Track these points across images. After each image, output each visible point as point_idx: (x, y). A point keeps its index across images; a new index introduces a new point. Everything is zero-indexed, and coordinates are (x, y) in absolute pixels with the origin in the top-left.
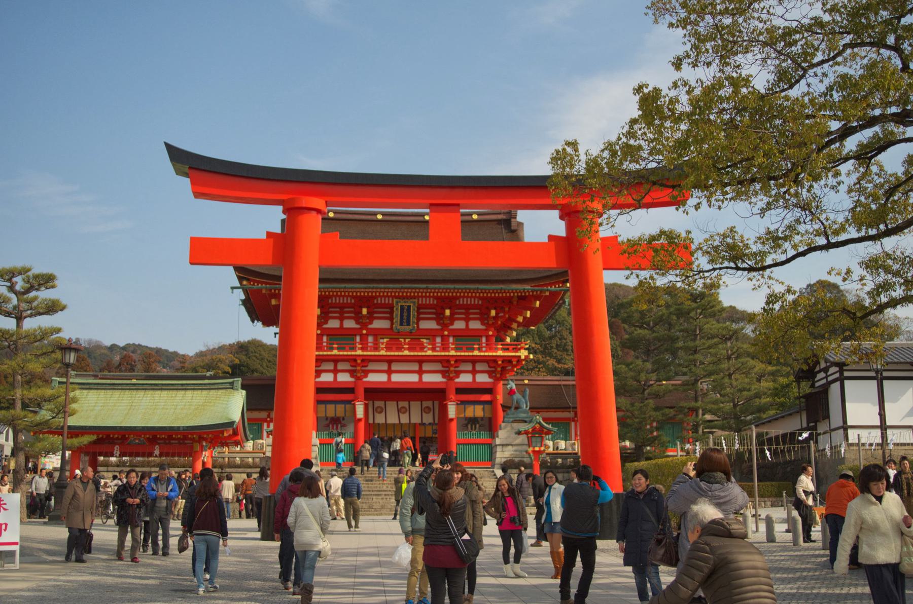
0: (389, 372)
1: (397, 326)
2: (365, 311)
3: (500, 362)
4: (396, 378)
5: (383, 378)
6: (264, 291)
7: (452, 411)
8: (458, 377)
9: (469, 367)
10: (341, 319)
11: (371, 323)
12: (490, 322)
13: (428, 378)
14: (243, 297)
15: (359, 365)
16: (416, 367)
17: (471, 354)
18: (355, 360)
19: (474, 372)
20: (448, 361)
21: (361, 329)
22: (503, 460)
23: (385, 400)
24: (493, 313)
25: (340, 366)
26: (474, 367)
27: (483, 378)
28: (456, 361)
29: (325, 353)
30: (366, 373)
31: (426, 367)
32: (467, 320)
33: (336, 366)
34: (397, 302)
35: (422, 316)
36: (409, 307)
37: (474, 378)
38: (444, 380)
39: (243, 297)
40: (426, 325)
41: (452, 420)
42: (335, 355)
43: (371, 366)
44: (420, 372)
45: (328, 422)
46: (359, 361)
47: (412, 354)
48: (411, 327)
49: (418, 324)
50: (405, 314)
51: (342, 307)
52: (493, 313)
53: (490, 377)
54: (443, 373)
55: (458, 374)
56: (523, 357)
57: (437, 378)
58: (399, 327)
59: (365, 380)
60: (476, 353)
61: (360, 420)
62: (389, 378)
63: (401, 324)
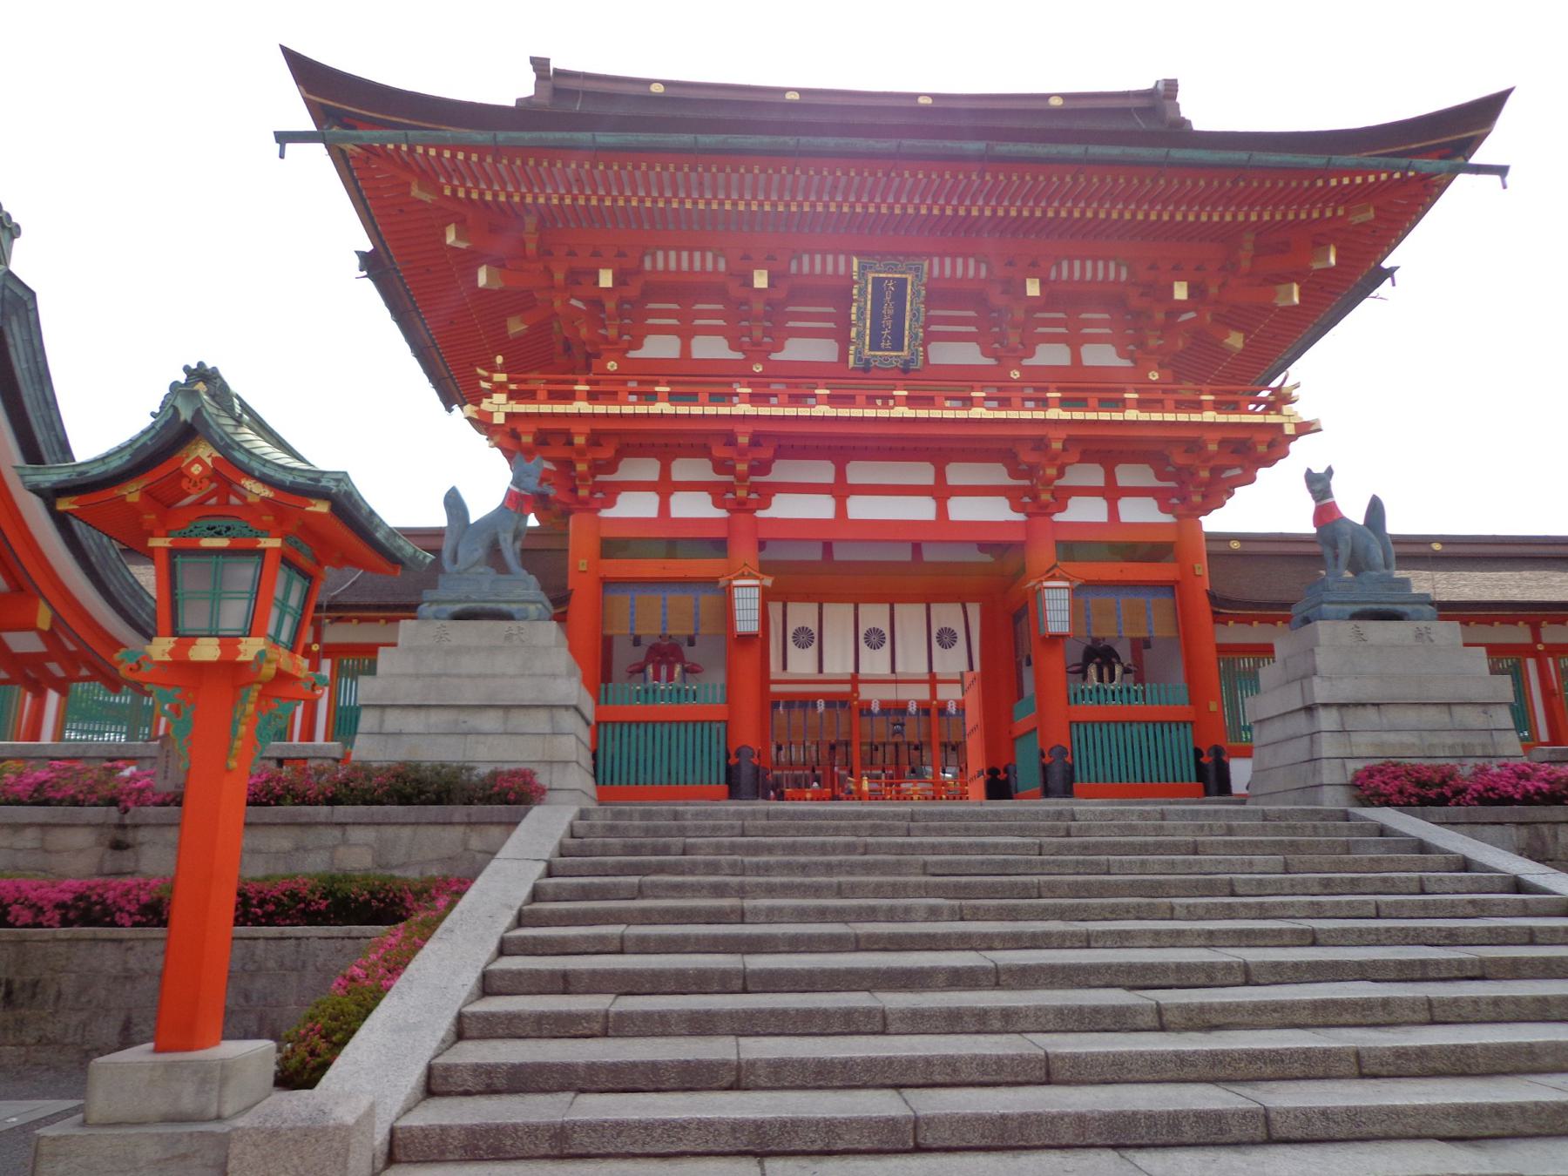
0: (841, 491)
1: (861, 348)
2: (761, 280)
3: (1213, 447)
4: (861, 508)
5: (820, 508)
6: (415, 192)
7: (1056, 610)
8: (1063, 508)
9: (1093, 475)
10: (686, 334)
11: (780, 348)
12: (1153, 343)
13: (963, 510)
14: (367, 246)
15: (742, 453)
16: (923, 474)
17: (1117, 416)
18: (730, 439)
19: (1112, 493)
20: (1041, 444)
21: (749, 361)
22: (1354, 766)
23: (820, 597)
24: (1181, 292)
25: (683, 469)
26: (1110, 477)
27: (1140, 512)
28: (1069, 442)
29: (627, 410)
30: (767, 493)
31: (957, 474)
32: (1075, 342)
33: (665, 471)
34: (863, 268)
35: (934, 328)
36: (902, 283)
37: (1113, 512)
38: (1020, 517)
39: (367, 246)
40: (947, 354)
41: (1056, 639)
42: (662, 416)
43: (783, 471)
44: (941, 492)
45: (640, 654)
46: (743, 440)
47: (923, 413)
48: (905, 353)
49: (925, 344)
50: (888, 310)
51: (683, 290)
52: (1181, 292)
53: (1164, 508)
54: (1013, 496)
55: (1062, 497)
56: (1289, 430)
57: (996, 510)
58: (867, 352)
59: (760, 514)
60: (1132, 415)
61: (746, 639)
62: (841, 509)
63: (875, 345)
